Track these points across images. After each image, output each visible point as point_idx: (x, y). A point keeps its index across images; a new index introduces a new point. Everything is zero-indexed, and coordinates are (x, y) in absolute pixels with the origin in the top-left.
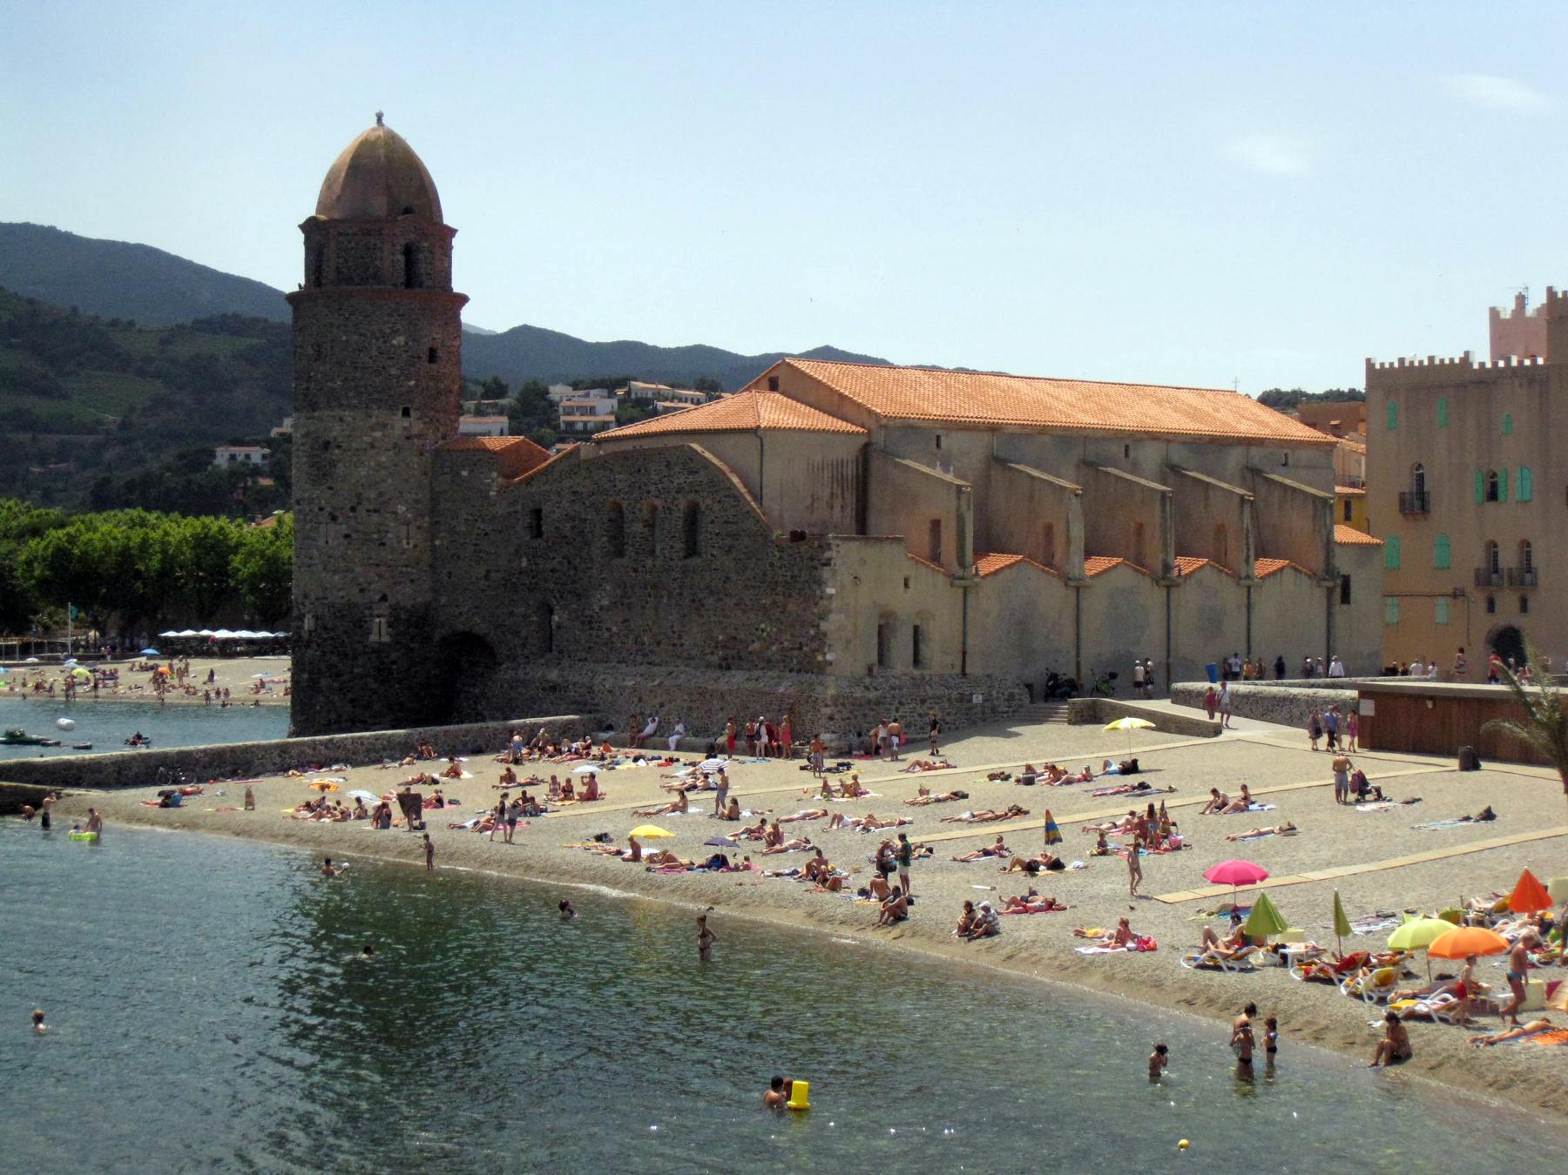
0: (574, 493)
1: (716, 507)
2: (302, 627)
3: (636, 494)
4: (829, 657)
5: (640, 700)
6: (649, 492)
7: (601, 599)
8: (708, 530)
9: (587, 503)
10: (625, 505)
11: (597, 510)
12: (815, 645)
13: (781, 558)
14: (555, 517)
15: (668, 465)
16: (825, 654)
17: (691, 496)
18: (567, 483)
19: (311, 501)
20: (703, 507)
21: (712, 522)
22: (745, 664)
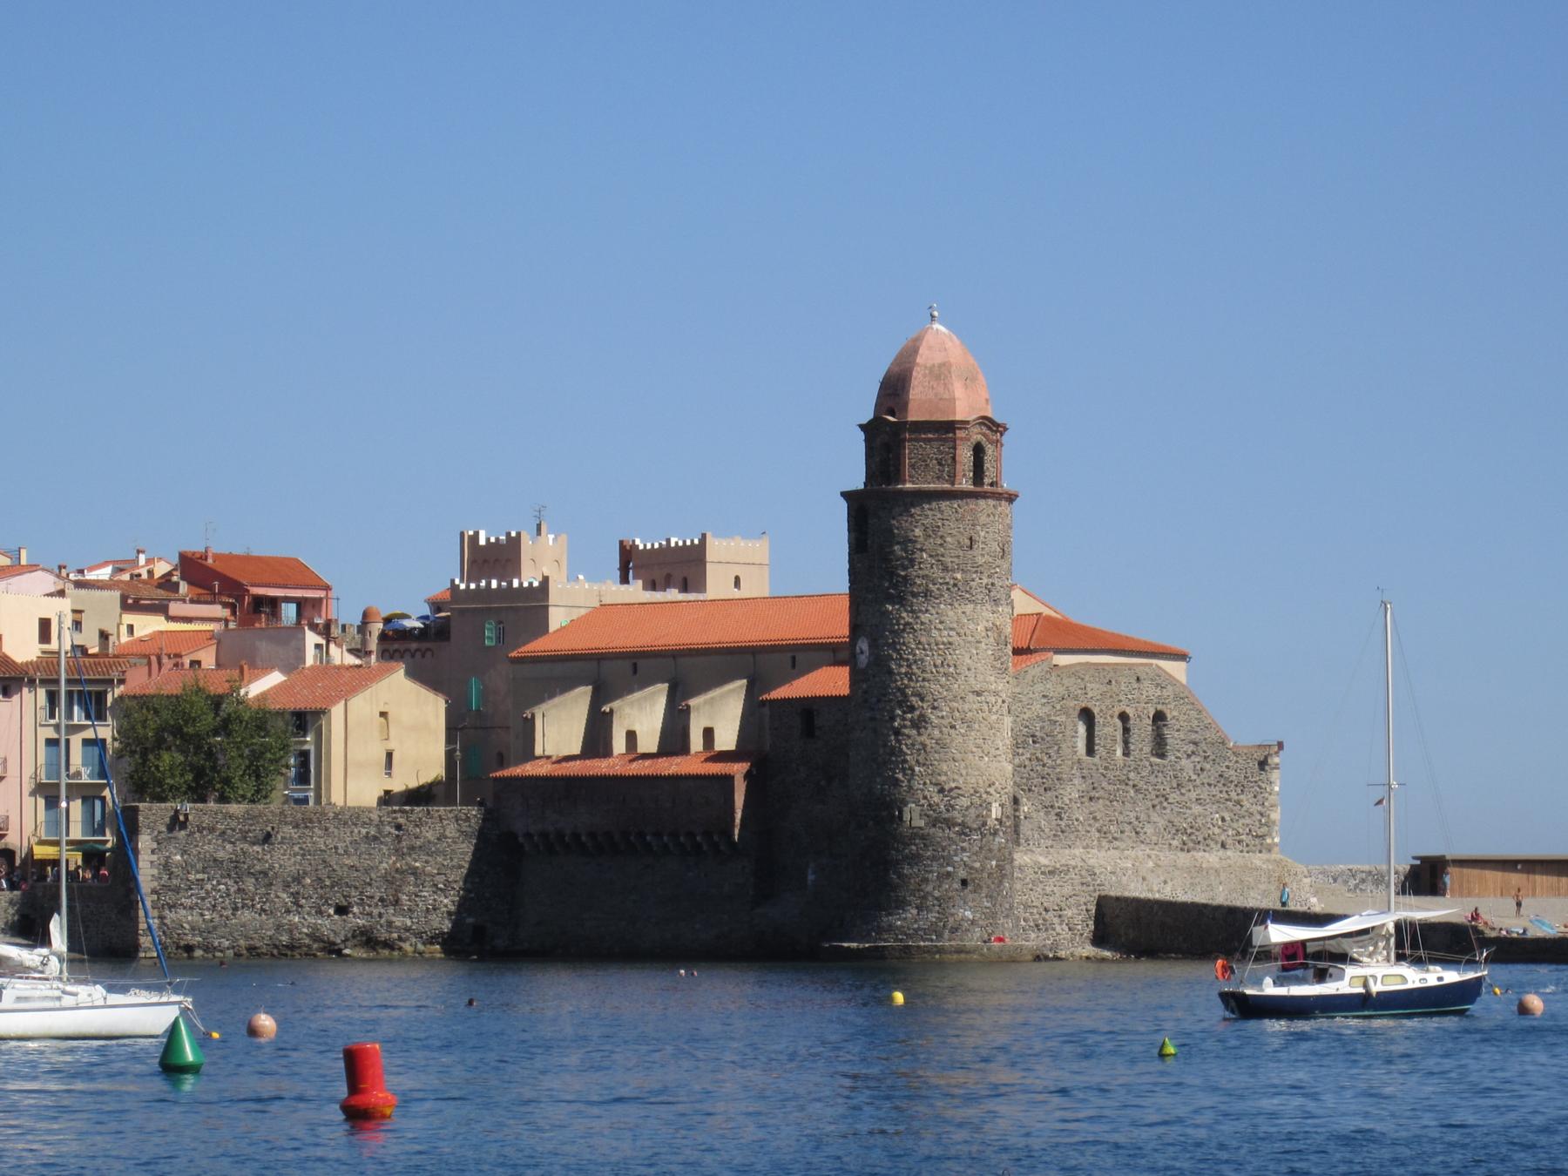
0: (1044, 696)
1: (1182, 718)
2: (990, 816)
3: (1108, 702)
4: (1277, 840)
5: (1144, 879)
6: (1120, 701)
7: (1071, 791)
8: (1173, 737)
9: (1058, 707)
10: (1096, 711)
11: (1068, 715)
12: (1264, 830)
13: (1237, 762)
14: (1026, 717)
15: (1138, 679)
16: (1273, 839)
17: (1160, 707)
18: (1039, 687)
19: (996, 693)
20: (1169, 716)
21: (1178, 730)
22: (1201, 847)
